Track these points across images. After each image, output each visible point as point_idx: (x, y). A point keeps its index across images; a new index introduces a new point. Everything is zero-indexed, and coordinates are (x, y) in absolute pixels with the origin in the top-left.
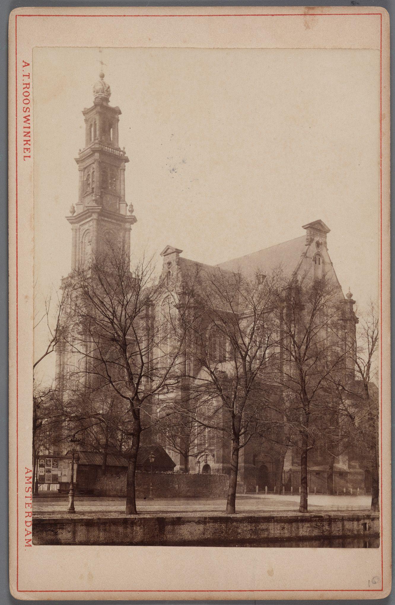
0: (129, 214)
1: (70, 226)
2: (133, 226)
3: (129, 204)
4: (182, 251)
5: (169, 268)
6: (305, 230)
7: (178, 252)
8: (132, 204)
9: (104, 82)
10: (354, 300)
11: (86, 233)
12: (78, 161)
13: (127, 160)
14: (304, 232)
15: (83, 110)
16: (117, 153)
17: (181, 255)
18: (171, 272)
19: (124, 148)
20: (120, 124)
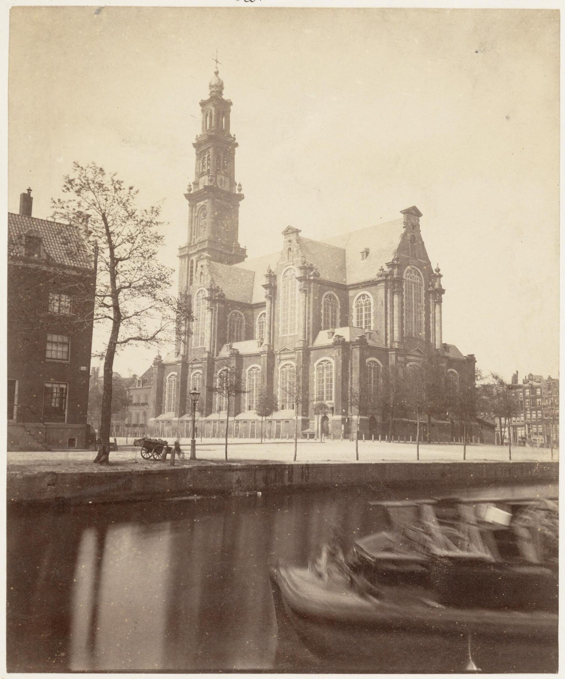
0: (237, 192)
2: (240, 203)
3: (238, 184)
4: (301, 231)
5: (290, 245)
6: (403, 215)
7: (297, 231)
8: (241, 184)
9: (219, 79)
12: (194, 145)
13: (237, 145)
14: (402, 216)
15: (200, 102)
18: (292, 249)
19: (234, 135)
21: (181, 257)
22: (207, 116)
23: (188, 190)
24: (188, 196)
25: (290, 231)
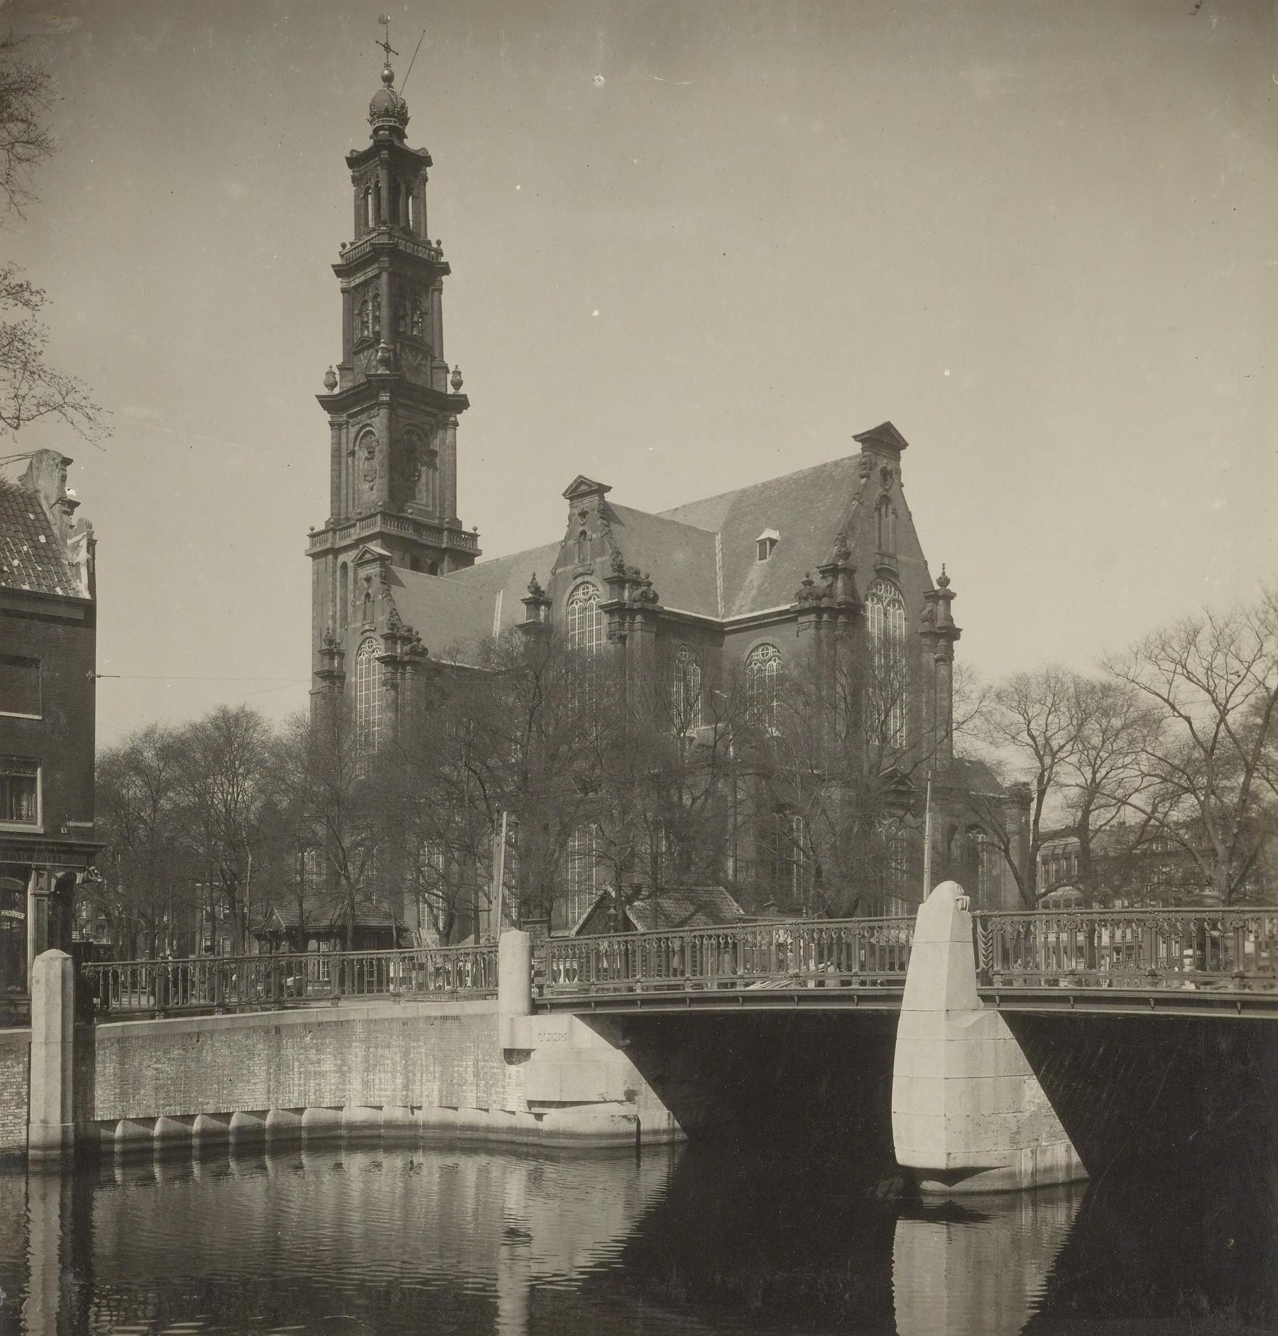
0: (451, 390)
1: (327, 417)
3: (452, 369)
4: (608, 489)
6: (860, 445)
7: (603, 489)
8: (460, 369)
10: (953, 591)
11: (362, 434)
12: (340, 271)
14: (857, 448)
16: (422, 254)
17: (608, 497)
20: (429, 187)
21: (315, 556)
22: (366, 193)
23: (327, 386)
24: (326, 403)
25: (583, 488)
